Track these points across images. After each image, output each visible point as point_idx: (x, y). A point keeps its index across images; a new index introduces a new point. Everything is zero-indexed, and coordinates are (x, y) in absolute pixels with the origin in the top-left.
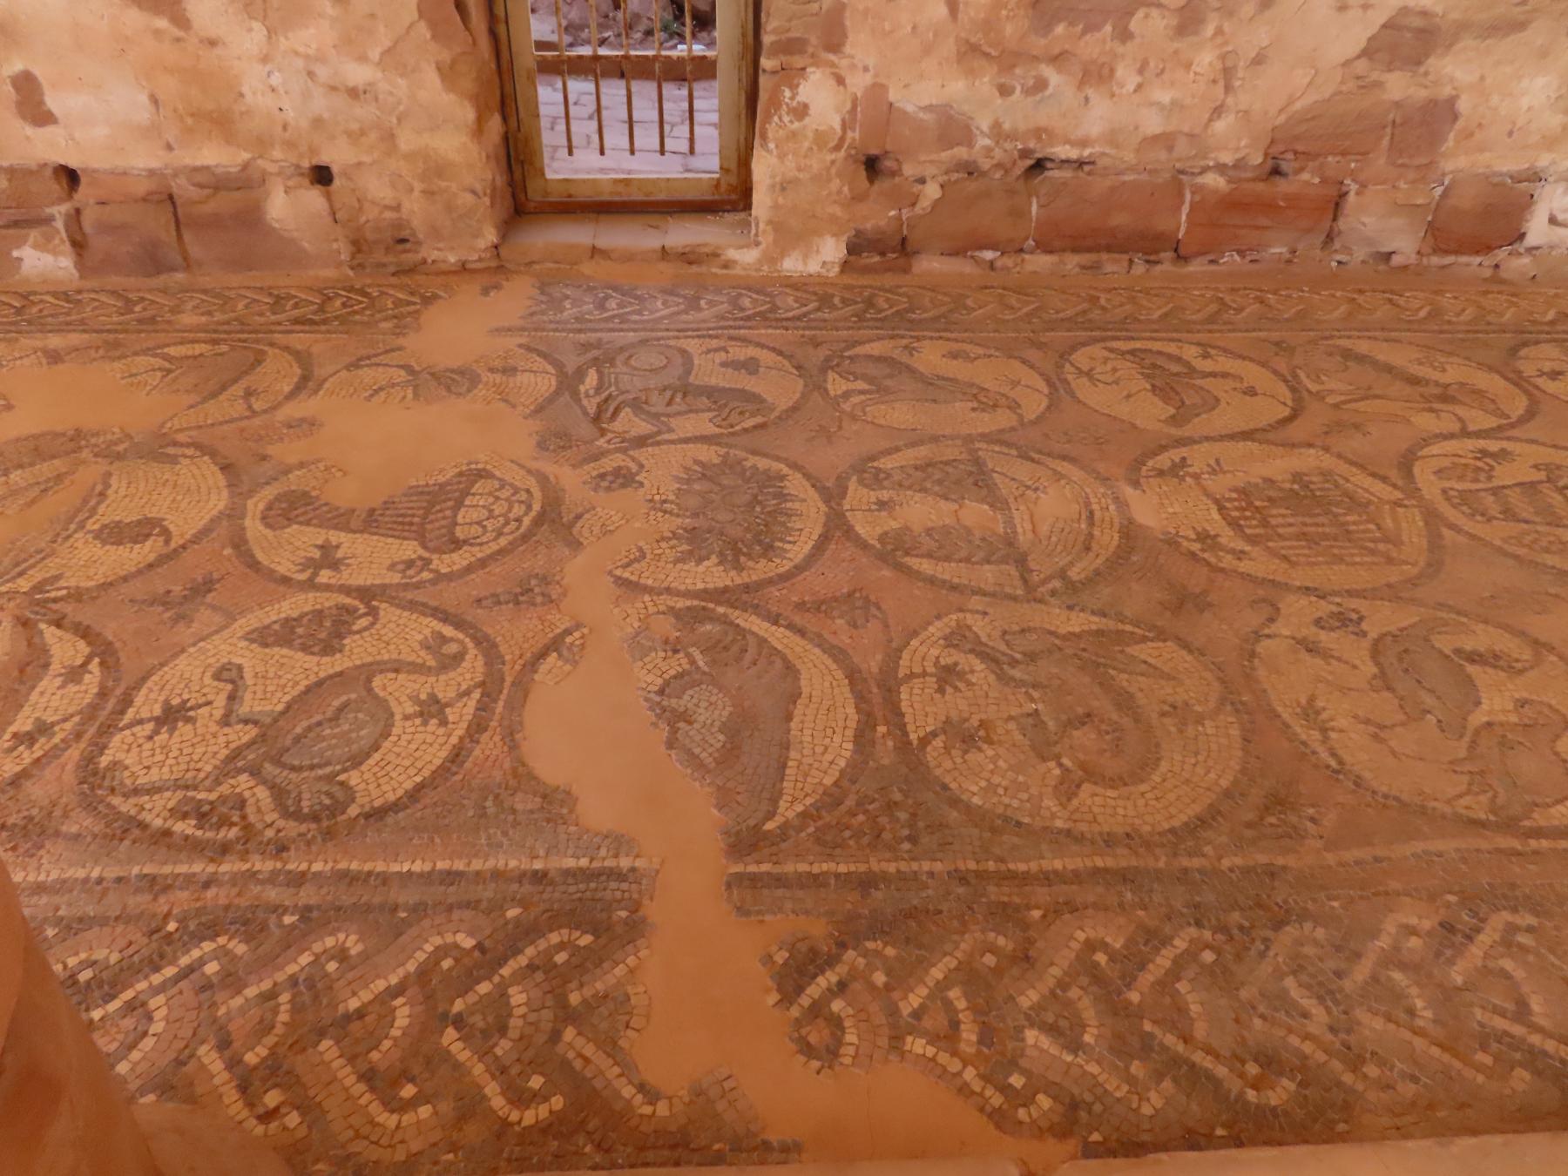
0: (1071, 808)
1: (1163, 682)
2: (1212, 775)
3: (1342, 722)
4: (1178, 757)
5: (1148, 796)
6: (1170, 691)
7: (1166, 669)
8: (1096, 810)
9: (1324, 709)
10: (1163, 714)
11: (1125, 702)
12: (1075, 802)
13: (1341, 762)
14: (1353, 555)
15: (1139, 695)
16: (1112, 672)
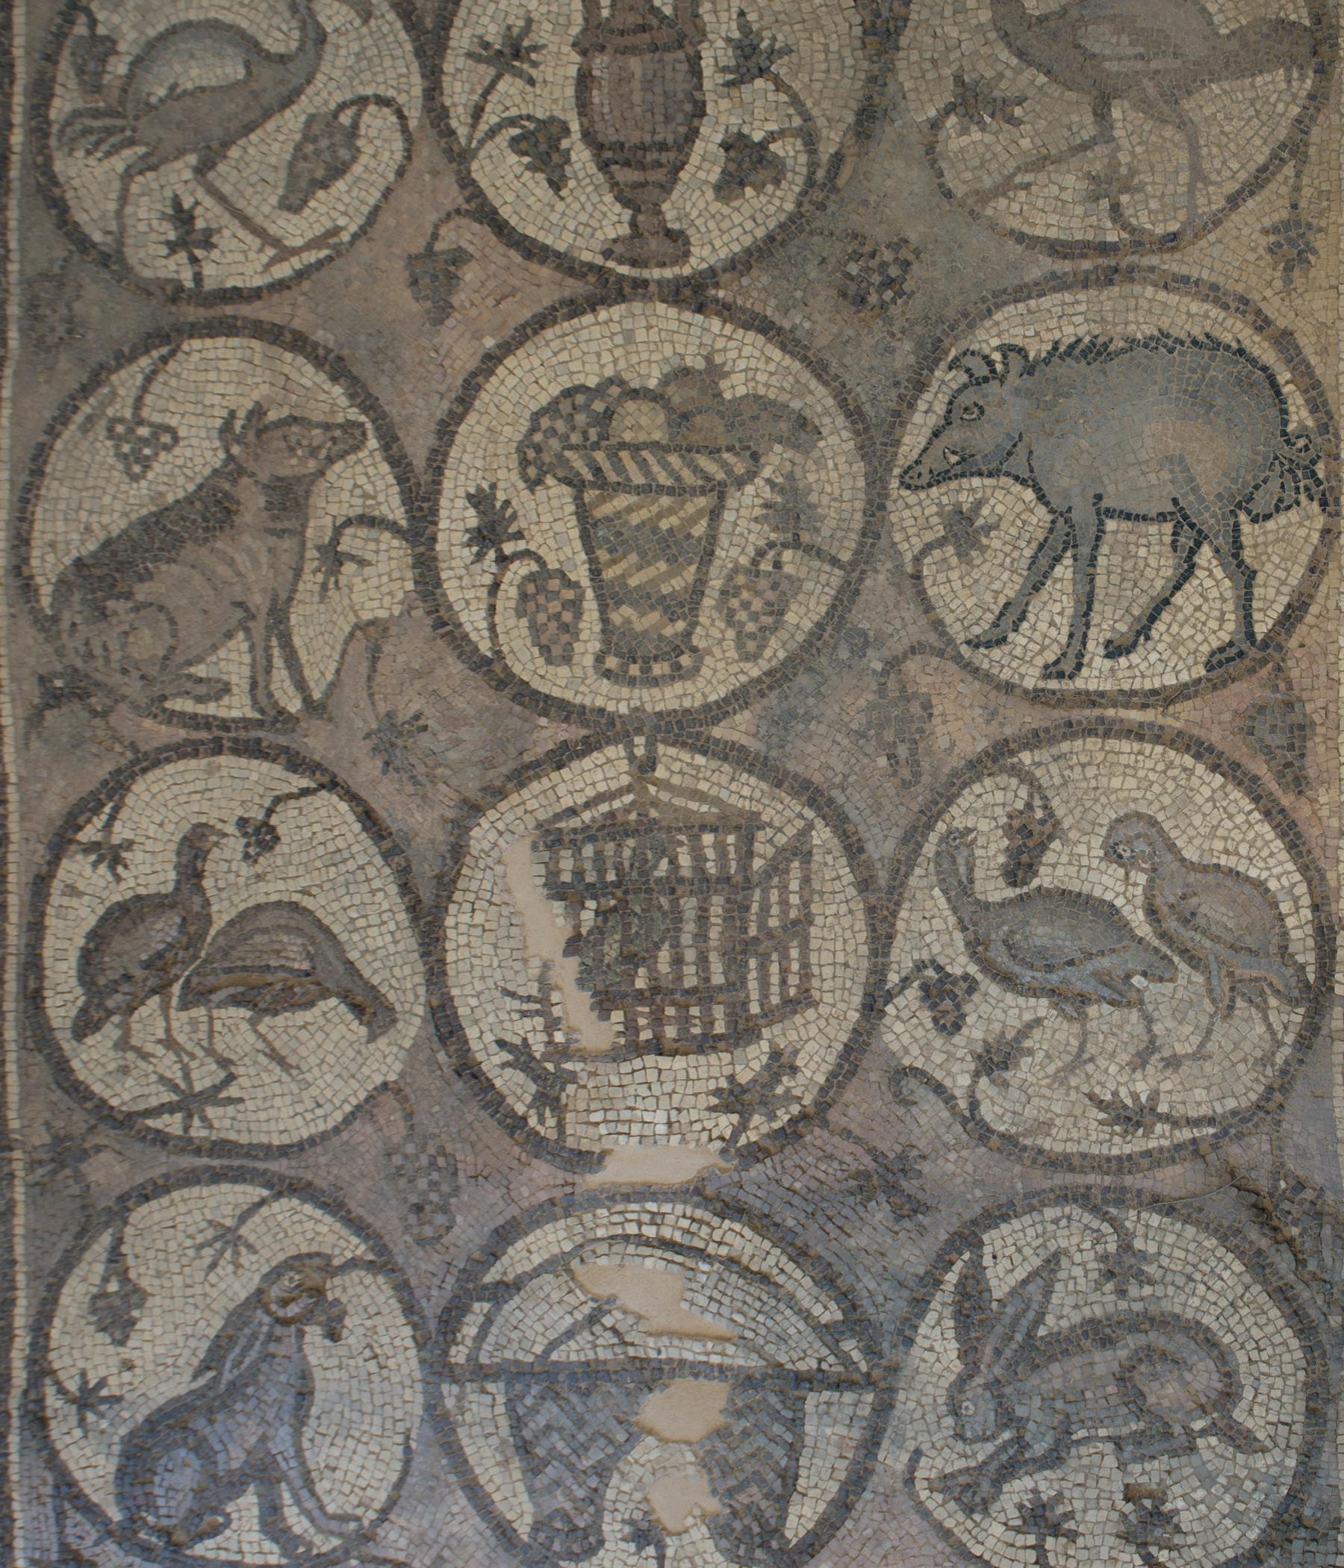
0: (1268, 1443)
1: (1062, 1275)
2: (1226, 1275)
3: (1143, 1089)
4: (1195, 1302)
5: (1254, 1355)
6: (1078, 1271)
7: (1037, 1262)
8: (1273, 1418)
9: (1115, 1094)
10: (1122, 1293)
11: (1099, 1333)
12: (1261, 1435)
13: (1211, 1121)
14: (784, 903)
15: (1087, 1312)
16: (1042, 1332)
